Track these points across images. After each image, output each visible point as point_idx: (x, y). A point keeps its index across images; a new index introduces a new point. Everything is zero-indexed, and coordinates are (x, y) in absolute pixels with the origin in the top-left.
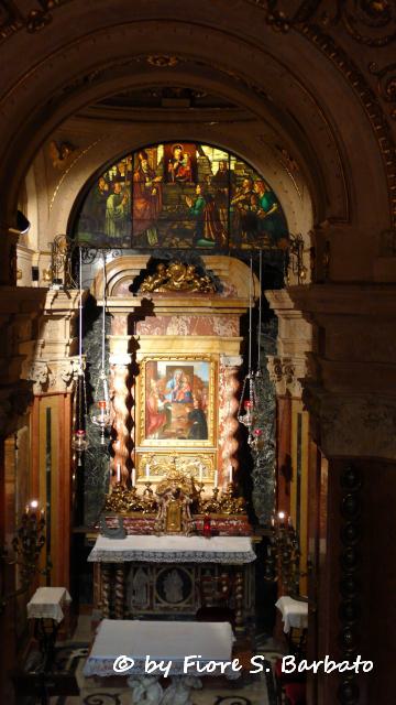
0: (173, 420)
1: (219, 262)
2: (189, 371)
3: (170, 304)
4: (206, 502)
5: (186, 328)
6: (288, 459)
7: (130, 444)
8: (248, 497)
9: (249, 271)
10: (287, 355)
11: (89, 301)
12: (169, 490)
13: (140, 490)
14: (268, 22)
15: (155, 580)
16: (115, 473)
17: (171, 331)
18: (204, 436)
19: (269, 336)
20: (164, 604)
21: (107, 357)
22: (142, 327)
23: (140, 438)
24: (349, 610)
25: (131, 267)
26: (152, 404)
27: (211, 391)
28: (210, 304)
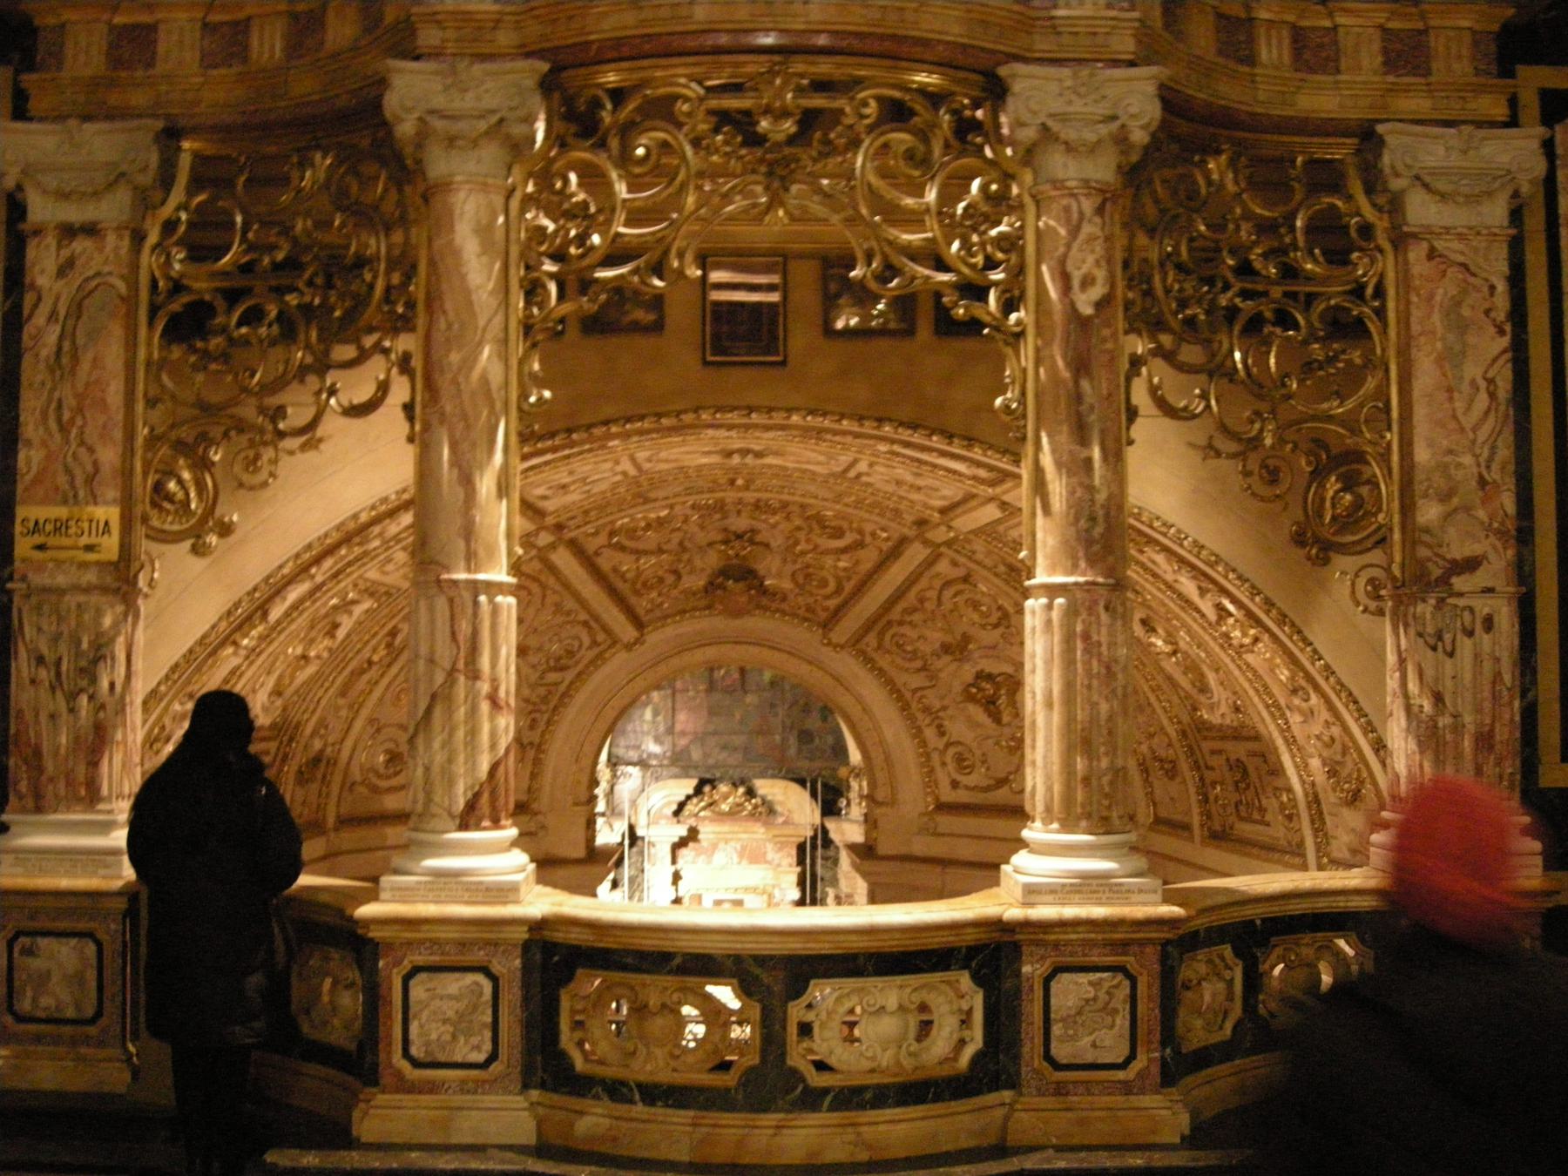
9: (805, 795)
11: (632, 828)
17: (720, 857)
19: (829, 863)
22: (685, 854)
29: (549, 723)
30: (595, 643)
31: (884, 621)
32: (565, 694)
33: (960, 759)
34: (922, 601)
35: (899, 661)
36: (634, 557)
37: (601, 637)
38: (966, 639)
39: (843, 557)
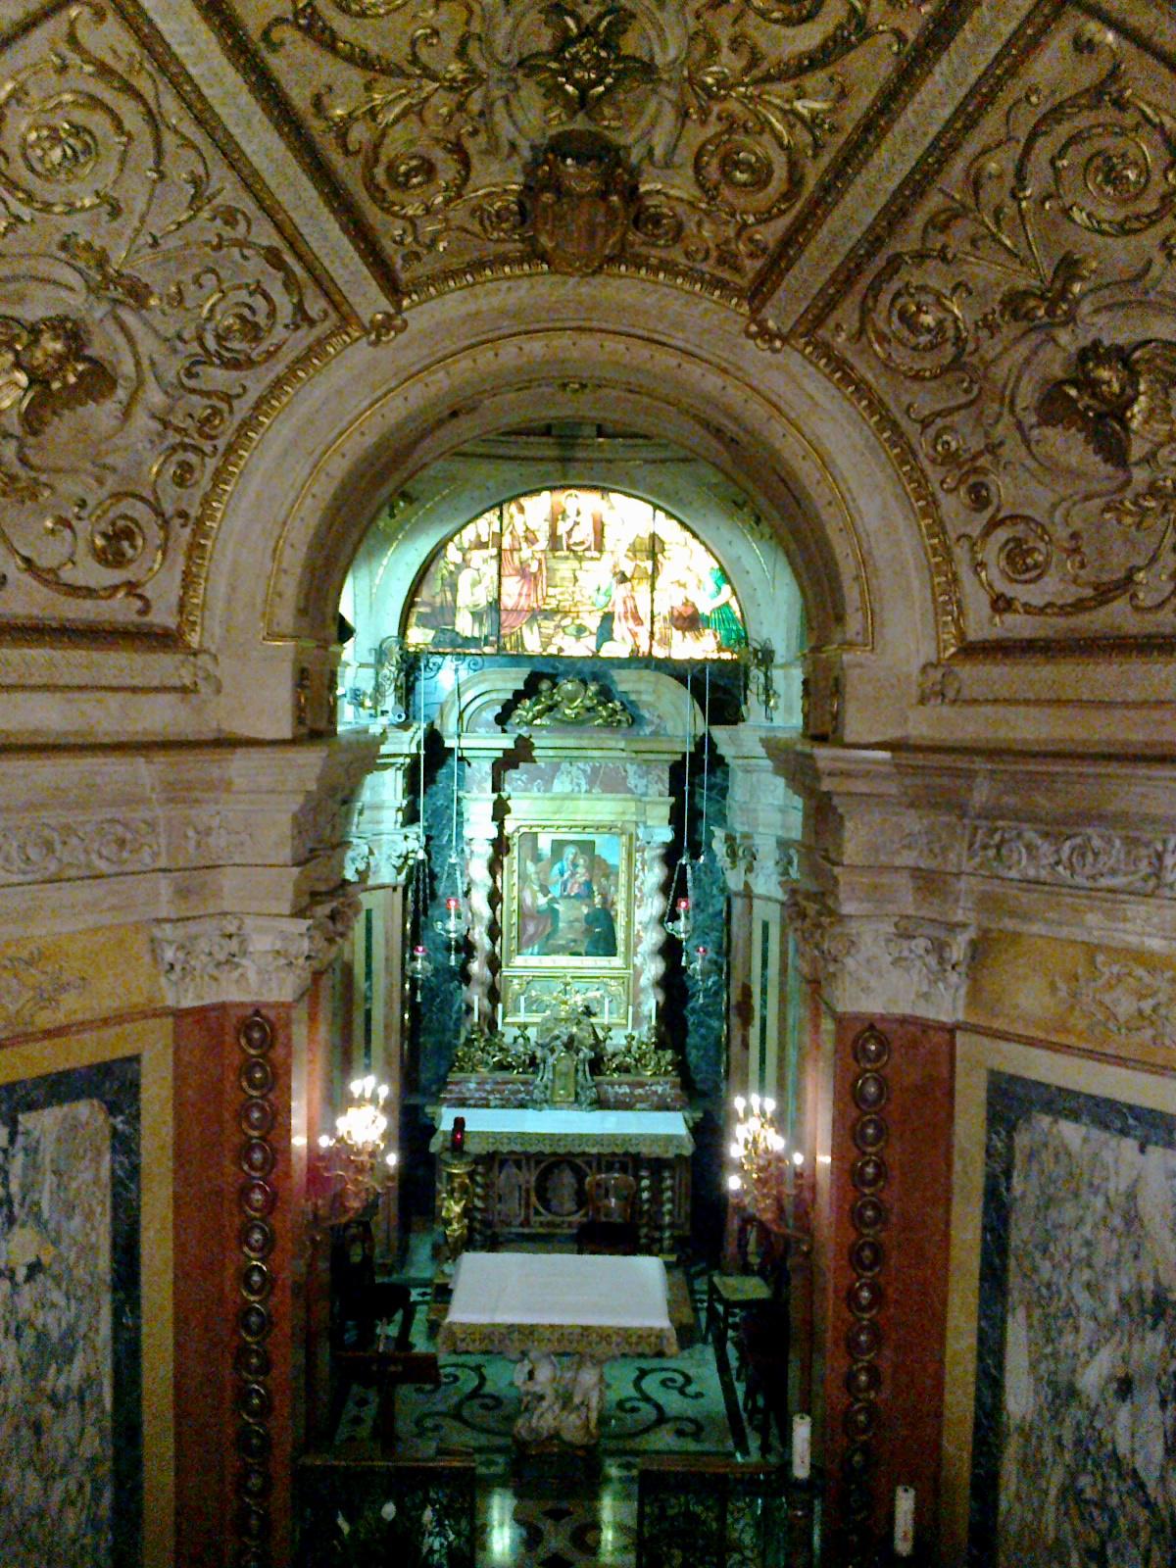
0: (561, 925)
1: (640, 680)
2: (587, 847)
3: (559, 743)
4: (614, 1055)
5: (583, 782)
6: (747, 992)
7: (494, 963)
8: (680, 1048)
9: (686, 694)
10: (746, 829)
11: (433, 739)
12: (557, 1038)
13: (509, 1034)
14: (749, 335)
15: (533, 1183)
16: (470, 1009)
17: (561, 785)
18: (611, 951)
20: (550, 1217)
21: (460, 825)
22: (514, 778)
23: (510, 953)
24: (867, 1253)
25: (499, 685)
26: (529, 901)
27: (623, 879)
28: (622, 745)
29: (219, 477)
30: (302, 317)
31: (880, 261)
32: (248, 424)
33: (1017, 556)
34: (976, 185)
35: (902, 357)
36: (356, 77)
37: (315, 306)
38: (1069, 268)
39: (815, 80)
